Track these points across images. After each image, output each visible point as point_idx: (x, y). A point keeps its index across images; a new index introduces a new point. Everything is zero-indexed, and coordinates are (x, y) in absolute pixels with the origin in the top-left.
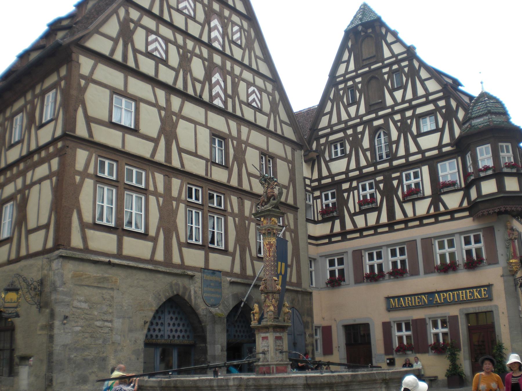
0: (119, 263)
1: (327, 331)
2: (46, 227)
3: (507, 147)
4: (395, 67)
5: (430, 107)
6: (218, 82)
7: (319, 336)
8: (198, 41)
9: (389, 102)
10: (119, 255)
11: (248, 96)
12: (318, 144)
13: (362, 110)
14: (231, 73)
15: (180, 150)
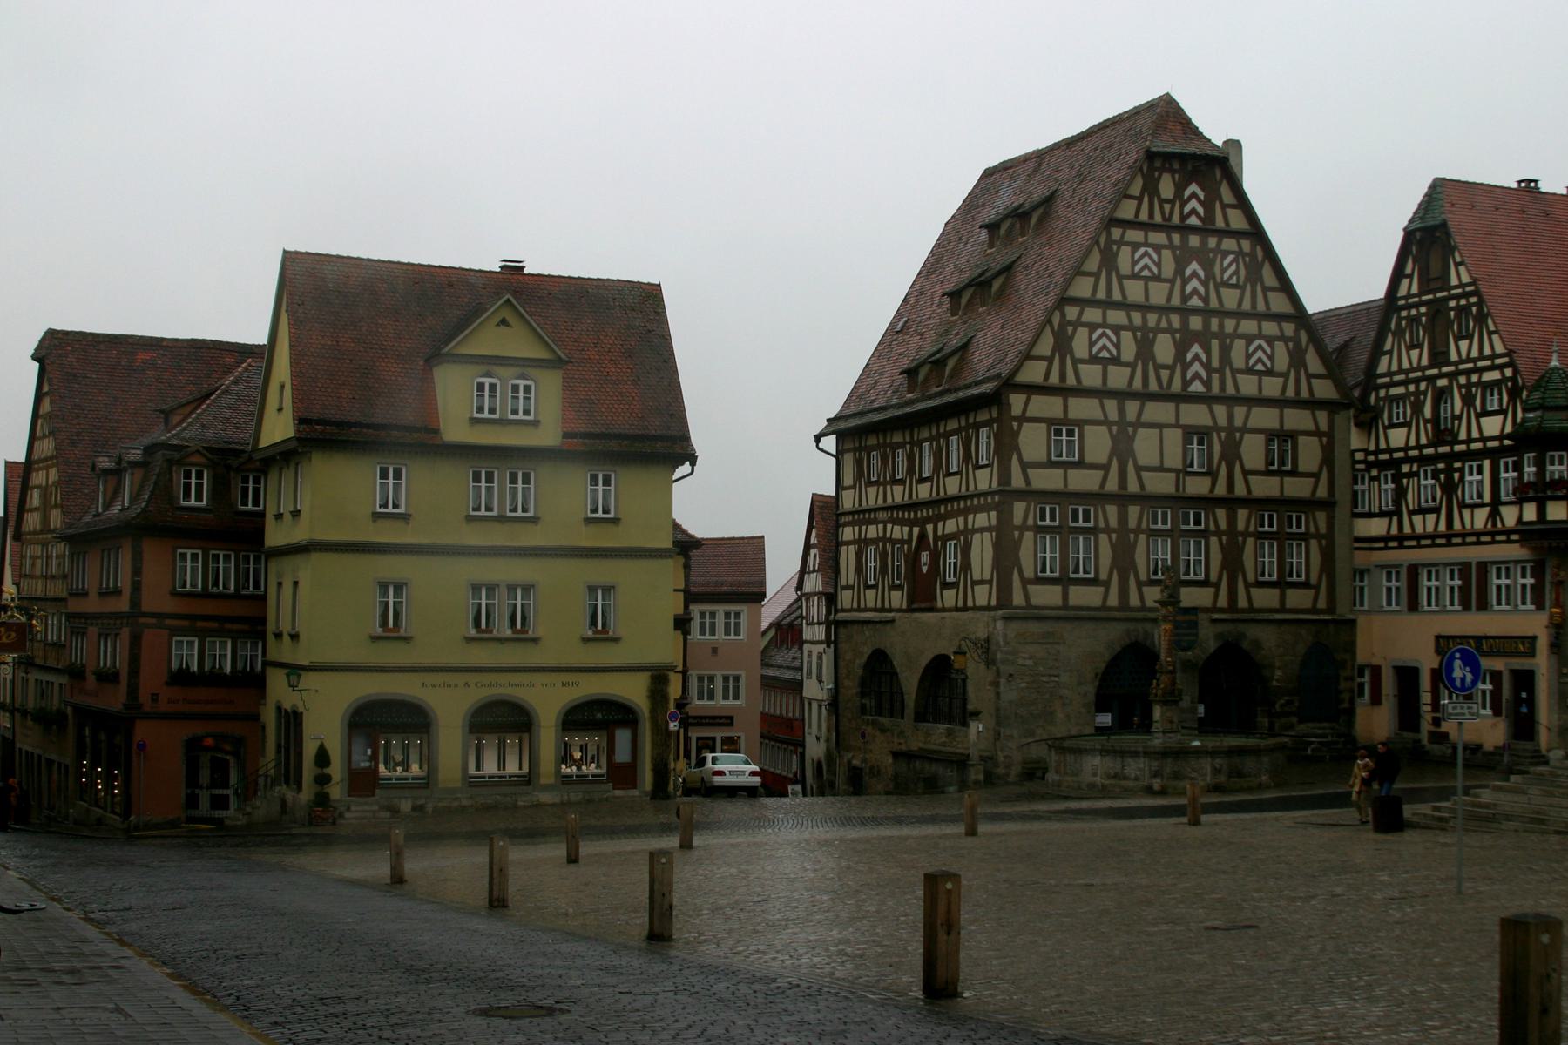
0: (1069, 615)
1: (1376, 671)
2: (990, 582)
3: (1561, 457)
4: (1463, 302)
5: (1495, 375)
6: (1196, 358)
7: (1366, 679)
8: (1164, 310)
9: (1454, 356)
10: (1065, 607)
11: (1248, 356)
12: (1378, 398)
13: (1425, 362)
14: (1221, 335)
15: (1139, 469)
